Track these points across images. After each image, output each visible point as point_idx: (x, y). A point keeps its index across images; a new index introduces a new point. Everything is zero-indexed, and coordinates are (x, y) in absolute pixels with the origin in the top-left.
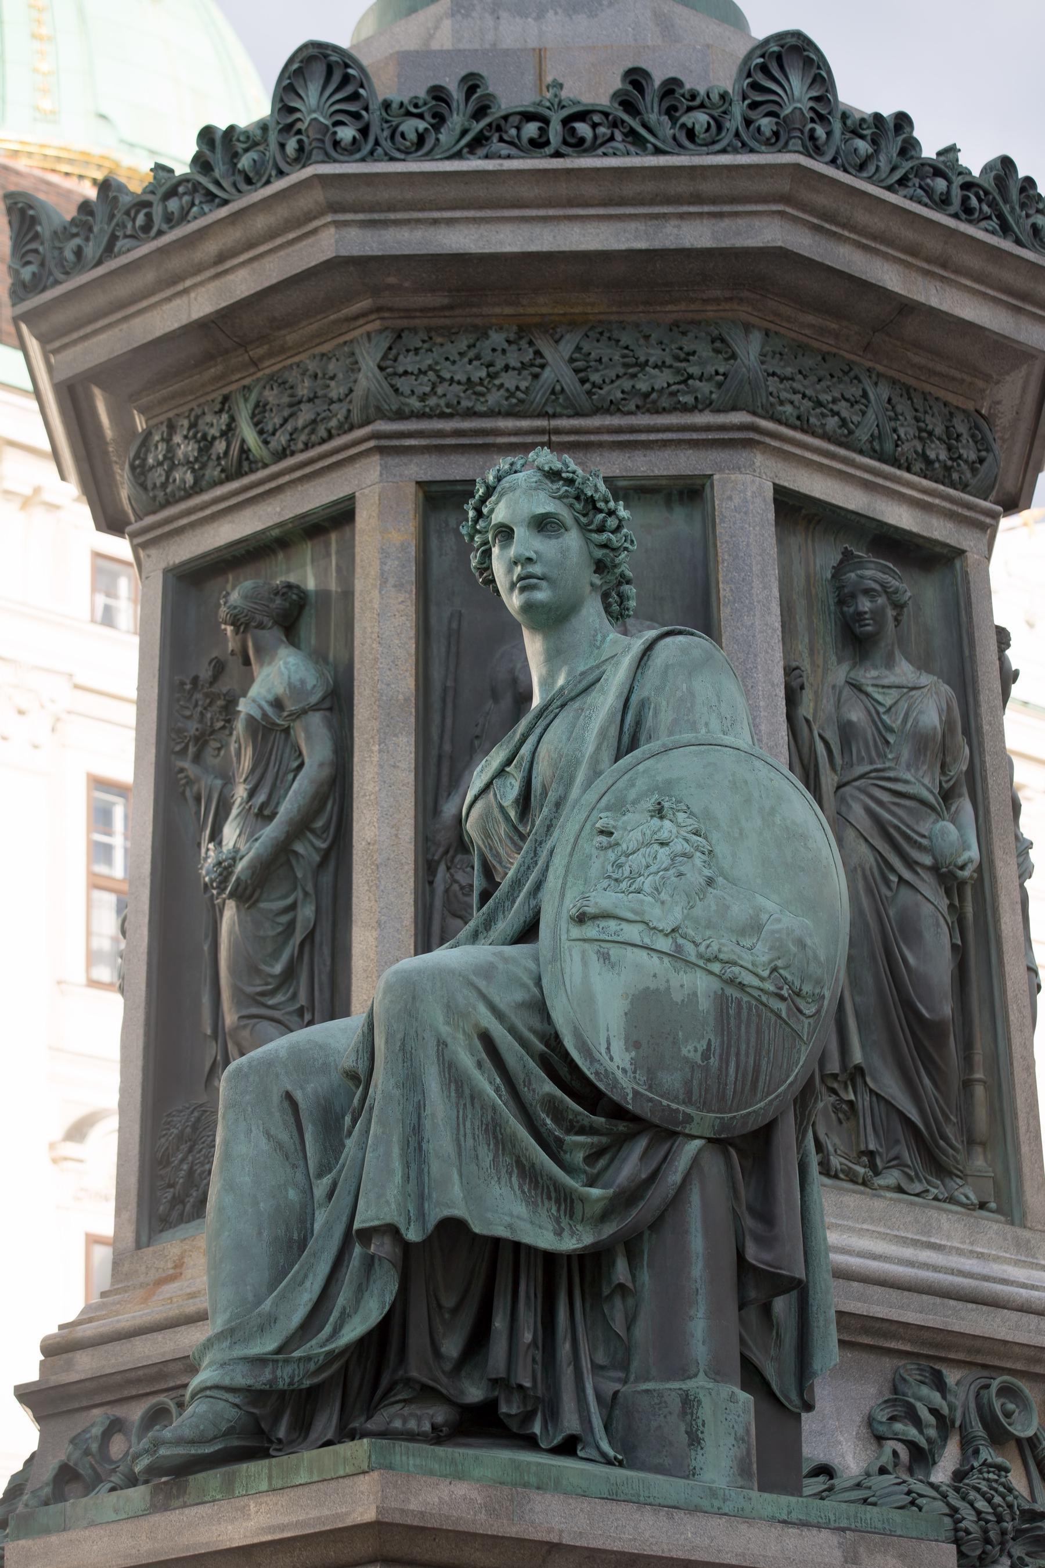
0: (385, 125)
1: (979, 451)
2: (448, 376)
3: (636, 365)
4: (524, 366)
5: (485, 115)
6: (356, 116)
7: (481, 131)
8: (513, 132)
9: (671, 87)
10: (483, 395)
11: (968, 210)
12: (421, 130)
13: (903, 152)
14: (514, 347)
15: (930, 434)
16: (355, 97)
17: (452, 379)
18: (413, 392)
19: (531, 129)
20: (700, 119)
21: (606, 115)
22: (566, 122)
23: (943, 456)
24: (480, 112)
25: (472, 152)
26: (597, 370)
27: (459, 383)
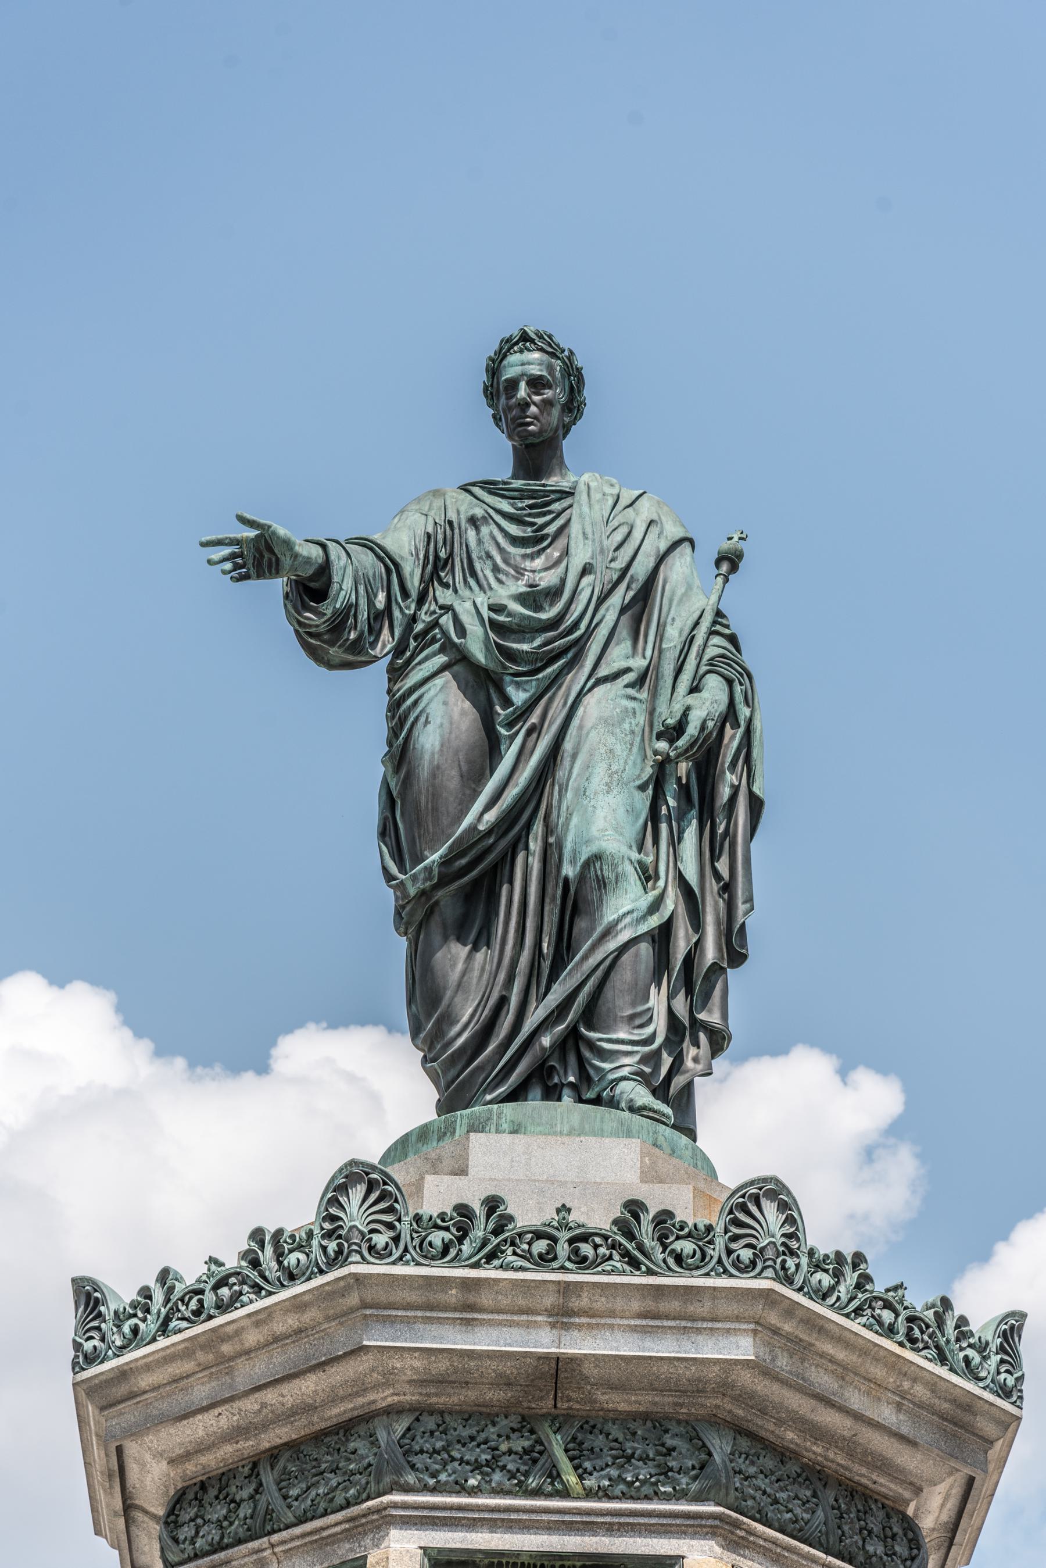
0: (415, 1235)
1: (911, 1549)
2: (458, 1456)
3: (623, 1457)
4: (526, 1451)
5: (503, 1231)
6: (390, 1226)
7: (498, 1244)
8: (526, 1247)
10: (488, 1474)
11: (913, 1341)
12: (446, 1240)
13: (859, 1286)
14: (517, 1434)
15: (870, 1532)
16: (391, 1210)
17: (462, 1458)
18: (427, 1469)
19: (541, 1246)
20: (686, 1247)
21: (606, 1238)
22: (571, 1241)
23: (880, 1550)
25: (487, 1263)
26: (589, 1459)
27: (468, 1463)
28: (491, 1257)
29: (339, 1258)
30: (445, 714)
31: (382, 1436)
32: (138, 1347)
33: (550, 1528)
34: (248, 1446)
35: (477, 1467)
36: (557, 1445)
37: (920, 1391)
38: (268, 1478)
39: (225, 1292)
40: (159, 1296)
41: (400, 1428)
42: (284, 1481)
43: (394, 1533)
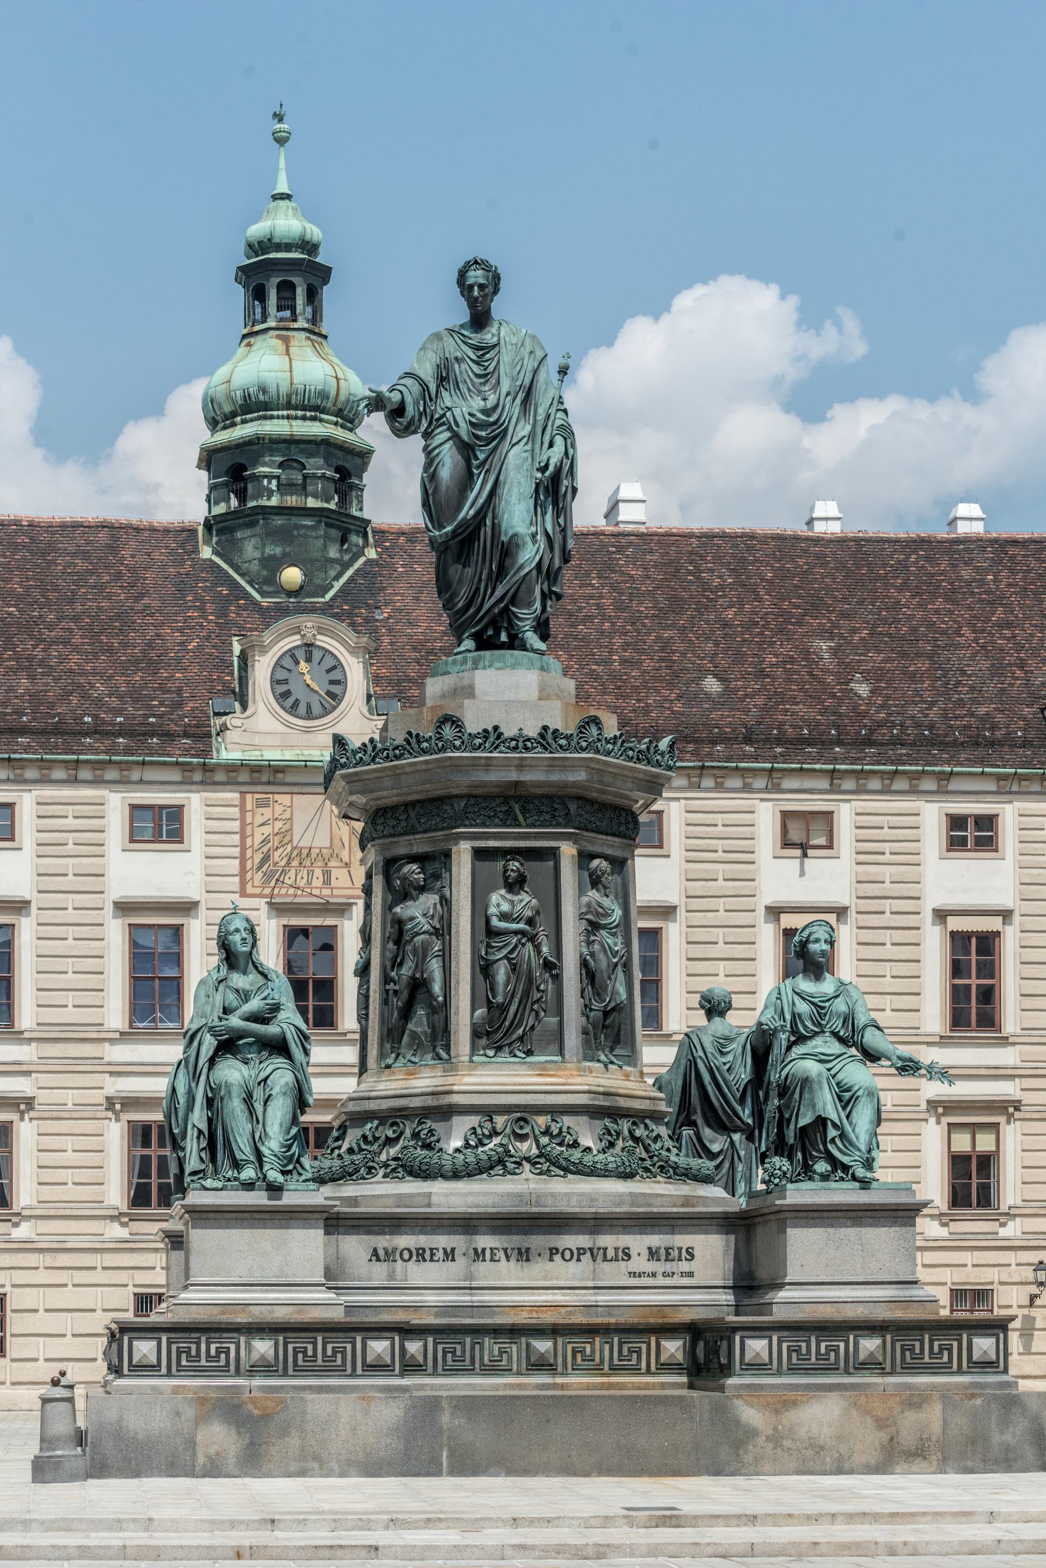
6: (460, 737)
9: (556, 731)
16: (460, 731)
20: (563, 742)
24: (498, 738)
28: (495, 748)
29: (443, 749)
30: (449, 460)
31: (456, 806)
32: (363, 765)
33: (515, 839)
34: (402, 799)
35: (490, 817)
36: (517, 808)
37: (641, 776)
38: (412, 814)
39: (397, 752)
40: (370, 748)
41: (463, 804)
42: (419, 816)
43: (462, 842)
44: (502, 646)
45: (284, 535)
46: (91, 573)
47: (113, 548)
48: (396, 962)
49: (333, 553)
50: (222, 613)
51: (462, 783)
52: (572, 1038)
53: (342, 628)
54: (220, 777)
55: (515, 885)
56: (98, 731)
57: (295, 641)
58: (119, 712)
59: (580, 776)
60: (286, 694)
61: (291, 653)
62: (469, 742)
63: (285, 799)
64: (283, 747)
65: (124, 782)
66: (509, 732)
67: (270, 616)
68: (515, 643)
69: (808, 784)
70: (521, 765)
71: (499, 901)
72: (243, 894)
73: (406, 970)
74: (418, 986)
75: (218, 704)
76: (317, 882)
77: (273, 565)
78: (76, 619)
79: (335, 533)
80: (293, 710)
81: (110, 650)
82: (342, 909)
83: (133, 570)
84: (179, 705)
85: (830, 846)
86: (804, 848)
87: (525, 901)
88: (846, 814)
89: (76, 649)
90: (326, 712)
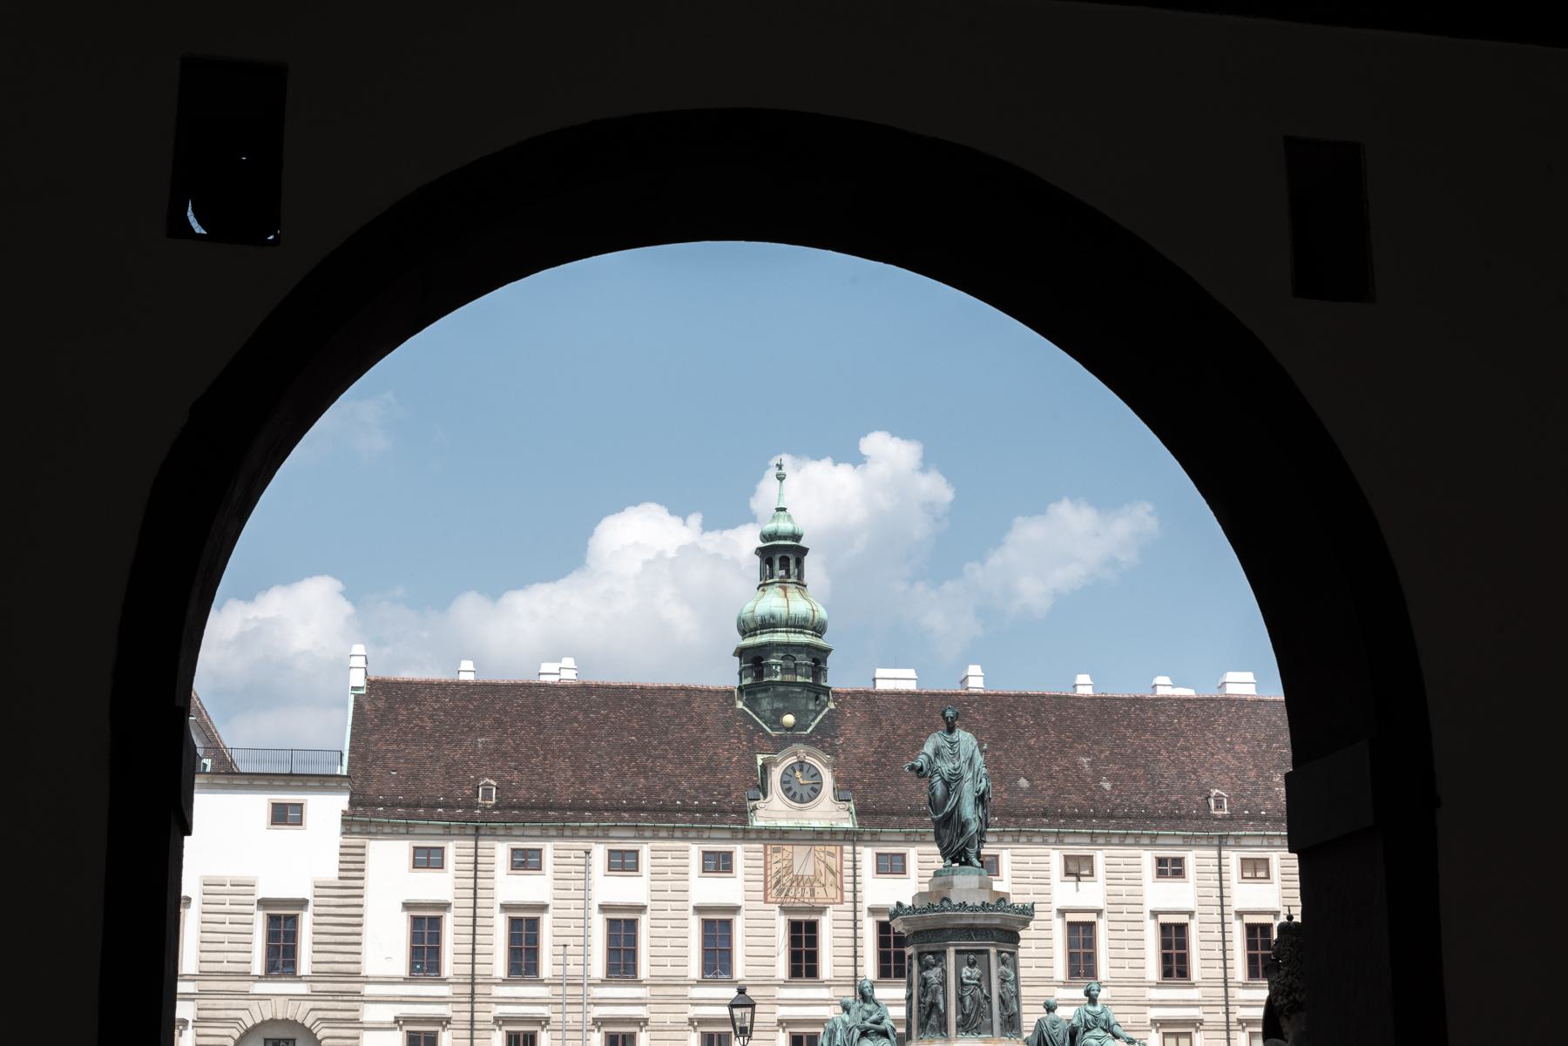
44: (961, 864)
45: (784, 697)
46: (677, 716)
47: (688, 702)
48: (924, 995)
49: (811, 706)
50: (750, 740)
51: (951, 923)
52: (996, 1027)
53: (820, 753)
54: (753, 835)
55: (972, 965)
56: (685, 809)
57: (793, 760)
58: (696, 798)
59: (997, 922)
60: (789, 789)
61: (792, 767)
62: (954, 908)
63: (789, 848)
64: (787, 819)
65: (699, 839)
66: (969, 904)
67: (779, 745)
68: (968, 862)
69: (1078, 840)
70: (974, 917)
71: (966, 971)
72: (766, 902)
73: (928, 999)
74: (934, 1005)
75: (751, 793)
76: (807, 895)
77: (779, 713)
78: (669, 743)
79: (812, 695)
80: (793, 798)
81: (689, 762)
82: (822, 911)
83: (700, 715)
84: (728, 794)
85: (1092, 875)
86: (1078, 876)
87: (976, 971)
88: (1100, 856)
89: (670, 762)
90: (811, 799)
